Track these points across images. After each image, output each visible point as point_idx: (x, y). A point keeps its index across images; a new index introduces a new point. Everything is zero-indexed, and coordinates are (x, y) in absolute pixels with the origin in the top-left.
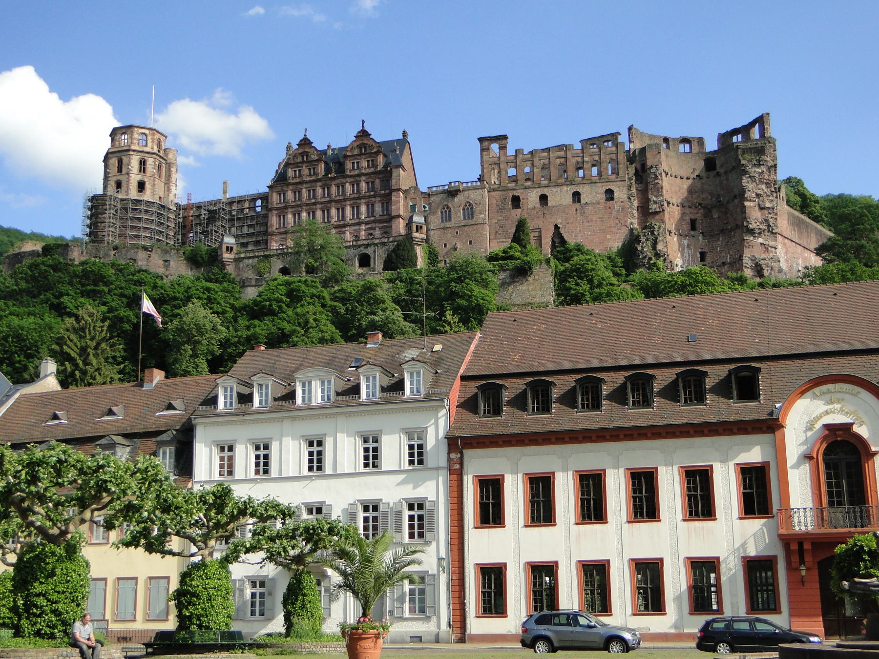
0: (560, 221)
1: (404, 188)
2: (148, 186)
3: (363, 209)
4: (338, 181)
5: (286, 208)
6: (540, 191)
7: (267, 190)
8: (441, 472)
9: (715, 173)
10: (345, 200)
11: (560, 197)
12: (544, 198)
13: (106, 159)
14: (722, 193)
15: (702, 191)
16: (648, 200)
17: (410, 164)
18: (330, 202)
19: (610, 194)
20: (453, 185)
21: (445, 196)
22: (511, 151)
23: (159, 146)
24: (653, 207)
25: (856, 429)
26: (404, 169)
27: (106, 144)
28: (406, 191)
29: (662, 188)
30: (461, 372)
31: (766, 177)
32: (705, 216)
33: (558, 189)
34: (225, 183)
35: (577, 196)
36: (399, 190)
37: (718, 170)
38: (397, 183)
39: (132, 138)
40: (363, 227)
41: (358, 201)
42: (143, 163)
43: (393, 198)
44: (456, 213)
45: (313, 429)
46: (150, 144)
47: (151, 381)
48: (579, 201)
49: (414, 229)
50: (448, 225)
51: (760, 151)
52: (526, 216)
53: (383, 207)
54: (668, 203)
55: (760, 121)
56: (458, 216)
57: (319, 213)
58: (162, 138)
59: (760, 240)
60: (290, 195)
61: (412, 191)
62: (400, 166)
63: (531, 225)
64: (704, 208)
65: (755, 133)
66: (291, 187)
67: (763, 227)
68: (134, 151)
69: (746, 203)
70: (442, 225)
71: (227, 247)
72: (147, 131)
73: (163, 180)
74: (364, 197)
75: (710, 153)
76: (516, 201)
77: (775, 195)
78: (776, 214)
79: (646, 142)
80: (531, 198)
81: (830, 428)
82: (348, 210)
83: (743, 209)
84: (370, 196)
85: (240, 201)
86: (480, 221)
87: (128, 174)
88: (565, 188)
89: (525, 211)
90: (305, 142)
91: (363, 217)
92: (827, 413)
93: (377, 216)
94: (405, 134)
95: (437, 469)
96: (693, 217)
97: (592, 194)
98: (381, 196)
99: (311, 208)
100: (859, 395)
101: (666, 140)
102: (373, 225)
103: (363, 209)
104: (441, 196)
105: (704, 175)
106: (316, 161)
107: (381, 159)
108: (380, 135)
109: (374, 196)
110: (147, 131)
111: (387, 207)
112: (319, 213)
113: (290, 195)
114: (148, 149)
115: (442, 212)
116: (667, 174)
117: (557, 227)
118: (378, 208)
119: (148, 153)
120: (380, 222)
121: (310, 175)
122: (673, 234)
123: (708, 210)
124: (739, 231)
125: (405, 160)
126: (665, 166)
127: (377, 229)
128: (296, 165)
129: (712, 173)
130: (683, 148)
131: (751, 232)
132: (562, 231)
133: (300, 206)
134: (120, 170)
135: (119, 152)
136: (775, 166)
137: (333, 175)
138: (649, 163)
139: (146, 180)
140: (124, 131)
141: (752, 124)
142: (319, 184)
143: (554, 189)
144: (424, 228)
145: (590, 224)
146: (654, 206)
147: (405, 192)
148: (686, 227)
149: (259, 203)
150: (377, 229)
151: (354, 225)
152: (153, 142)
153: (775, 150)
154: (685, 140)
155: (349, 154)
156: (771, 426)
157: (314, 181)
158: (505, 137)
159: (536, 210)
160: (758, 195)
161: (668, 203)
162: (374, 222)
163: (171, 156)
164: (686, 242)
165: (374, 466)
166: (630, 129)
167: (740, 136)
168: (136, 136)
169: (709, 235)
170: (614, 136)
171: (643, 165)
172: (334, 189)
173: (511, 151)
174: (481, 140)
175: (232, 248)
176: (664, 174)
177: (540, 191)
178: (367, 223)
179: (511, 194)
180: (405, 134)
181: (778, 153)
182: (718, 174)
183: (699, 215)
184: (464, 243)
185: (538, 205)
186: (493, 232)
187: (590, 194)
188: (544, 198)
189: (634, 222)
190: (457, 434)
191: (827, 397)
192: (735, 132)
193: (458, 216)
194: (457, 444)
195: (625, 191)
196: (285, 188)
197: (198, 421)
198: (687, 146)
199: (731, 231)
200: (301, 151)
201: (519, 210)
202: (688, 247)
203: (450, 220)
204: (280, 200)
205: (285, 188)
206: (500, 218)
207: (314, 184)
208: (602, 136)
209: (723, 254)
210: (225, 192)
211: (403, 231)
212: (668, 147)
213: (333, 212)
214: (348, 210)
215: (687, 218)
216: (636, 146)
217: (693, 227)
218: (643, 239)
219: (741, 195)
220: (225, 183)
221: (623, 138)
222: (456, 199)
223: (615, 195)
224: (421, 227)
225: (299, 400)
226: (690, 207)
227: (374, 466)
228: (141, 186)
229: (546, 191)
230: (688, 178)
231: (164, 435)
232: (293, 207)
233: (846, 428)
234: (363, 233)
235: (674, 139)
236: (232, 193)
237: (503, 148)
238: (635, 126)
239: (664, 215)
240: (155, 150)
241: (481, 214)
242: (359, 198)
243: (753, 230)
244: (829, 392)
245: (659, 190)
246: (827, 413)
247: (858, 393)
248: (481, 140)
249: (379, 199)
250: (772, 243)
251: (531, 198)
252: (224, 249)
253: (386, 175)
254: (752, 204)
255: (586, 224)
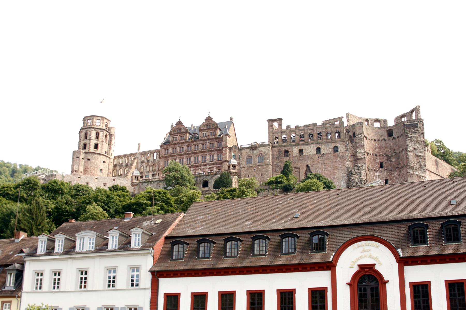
0: (309, 163)
1: (229, 146)
2: (99, 146)
3: (208, 157)
4: (195, 143)
5: (168, 157)
6: (299, 147)
7: (159, 148)
8: (147, 290)
9: (392, 137)
10: (199, 153)
11: (310, 150)
12: (301, 151)
13: (80, 133)
14: (396, 148)
15: (386, 147)
16: (356, 152)
17: (234, 134)
18: (191, 153)
19: (336, 149)
20: (253, 144)
21: (248, 150)
22: (284, 127)
23: (107, 126)
24: (359, 155)
25: (377, 268)
26: (229, 136)
27: (81, 125)
28: (231, 148)
29: (364, 145)
30: (166, 234)
31: (419, 139)
32: (388, 160)
33: (309, 146)
34: (139, 144)
35: (318, 150)
36: (227, 147)
37: (394, 136)
38: (226, 143)
39: (93, 122)
40: (207, 167)
41: (206, 153)
42: (97, 134)
43: (224, 152)
44: (254, 159)
45: (83, 264)
46: (101, 125)
47: (19, 238)
48: (320, 152)
49: (231, 167)
50: (250, 165)
51: (416, 126)
52: (292, 160)
53: (218, 156)
54: (368, 154)
55: (416, 110)
56: (256, 161)
57: (185, 160)
58: (108, 122)
59: (417, 173)
60: (170, 150)
61: (234, 148)
62: (227, 135)
63: (293, 166)
64: (387, 156)
65: (414, 117)
66: (172, 146)
67: (417, 166)
68: (93, 128)
69: (409, 154)
70: (247, 165)
71: (135, 177)
72: (100, 118)
73: (108, 143)
74: (209, 151)
75: (390, 127)
76: (286, 152)
77: (424, 149)
78: (425, 159)
79: (356, 121)
80: (295, 151)
81: (362, 267)
82: (200, 158)
83: (407, 158)
84: (212, 151)
85: (145, 154)
86: (267, 163)
87: (90, 140)
88: (312, 146)
89: (291, 158)
90: (179, 123)
91: (207, 162)
92: (361, 257)
93: (215, 161)
94: (231, 119)
95: (145, 289)
96: (381, 161)
97: (326, 149)
98: (217, 150)
99: (180, 156)
100: (379, 248)
101: (367, 120)
102: (213, 166)
103: (208, 157)
104: (247, 150)
105: (386, 138)
106: (184, 132)
107: (218, 132)
108: (217, 119)
109: (214, 151)
110: (100, 118)
111: (220, 156)
112: (185, 160)
113: (170, 150)
114: (100, 127)
115: (247, 159)
116: (366, 138)
117: (308, 166)
118: (216, 157)
119: (100, 129)
120: (216, 164)
121: (181, 140)
122: (370, 170)
123: (389, 158)
124: (405, 168)
125: (230, 132)
126: (365, 134)
127: (215, 168)
128: (175, 135)
129: (391, 138)
130: (377, 125)
131: (412, 168)
132: (311, 169)
133: (175, 156)
134: (86, 138)
135: (86, 128)
136: (423, 134)
137: (193, 140)
138: (357, 133)
139: (99, 142)
140: (89, 118)
141: (412, 112)
142: (185, 144)
143: (306, 147)
144: (237, 167)
145: (326, 164)
146: (360, 155)
147: (230, 149)
148: (377, 166)
149: (155, 154)
150: (215, 168)
151: (203, 165)
152: (103, 124)
153: (423, 125)
154: (377, 121)
155: (202, 128)
156: (330, 266)
157: (183, 143)
158: (281, 120)
159: (297, 157)
160: (415, 149)
161: (368, 154)
162: (214, 164)
163: (112, 131)
164: (377, 174)
165: (113, 287)
166: (347, 114)
167: (406, 118)
168: (95, 120)
169: (390, 171)
170: (340, 119)
171: (354, 134)
172: (193, 147)
173: (284, 127)
174: (268, 121)
175: (138, 177)
176: (365, 138)
177: (299, 147)
178: (209, 165)
179: (284, 149)
180: (231, 119)
181: (424, 126)
182: (394, 138)
183: (384, 160)
184: (258, 175)
185: (298, 155)
186: (274, 169)
187: (325, 149)
188: (301, 151)
189: (349, 164)
190: (156, 269)
191: (361, 249)
192: (403, 116)
193: (256, 161)
194: (156, 275)
195: (344, 147)
196: (168, 147)
197: (26, 259)
198: (378, 124)
199: (401, 168)
200: (177, 127)
201: (288, 157)
202: (379, 177)
203: (251, 163)
204: (165, 153)
205: (168, 147)
206: (278, 162)
207: (183, 144)
208: (334, 119)
209: (397, 181)
210: (139, 149)
211: (227, 168)
212: (368, 124)
213: (192, 159)
214: (200, 158)
215: (378, 161)
216: (351, 123)
217: (381, 166)
218: (353, 172)
219: (406, 149)
220: (139, 144)
221: (344, 120)
222: (255, 152)
223: (339, 149)
224: (235, 166)
225: (77, 249)
226: (379, 156)
227: (113, 287)
228: (96, 146)
229: (302, 147)
230: (379, 140)
231: (11, 266)
232: (172, 156)
233: (371, 267)
234: (207, 170)
235: (371, 120)
236: (142, 150)
237: (280, 125)
238: (350, 113)
239: (365, 160)
240: (104, 128)
241: (268, 159)
242: (206, 152)
243: (412, 167)
244: (362, 245)
245: (363, 146)
246: (361, 257)
247: (378, 246)
248: (268, 121)
249: (216, 152)
250: (423, 175)
251: (295, 151)
252: (134, 177)
253: (220, 139)
254: (411, 154)
255: (324, 165)
